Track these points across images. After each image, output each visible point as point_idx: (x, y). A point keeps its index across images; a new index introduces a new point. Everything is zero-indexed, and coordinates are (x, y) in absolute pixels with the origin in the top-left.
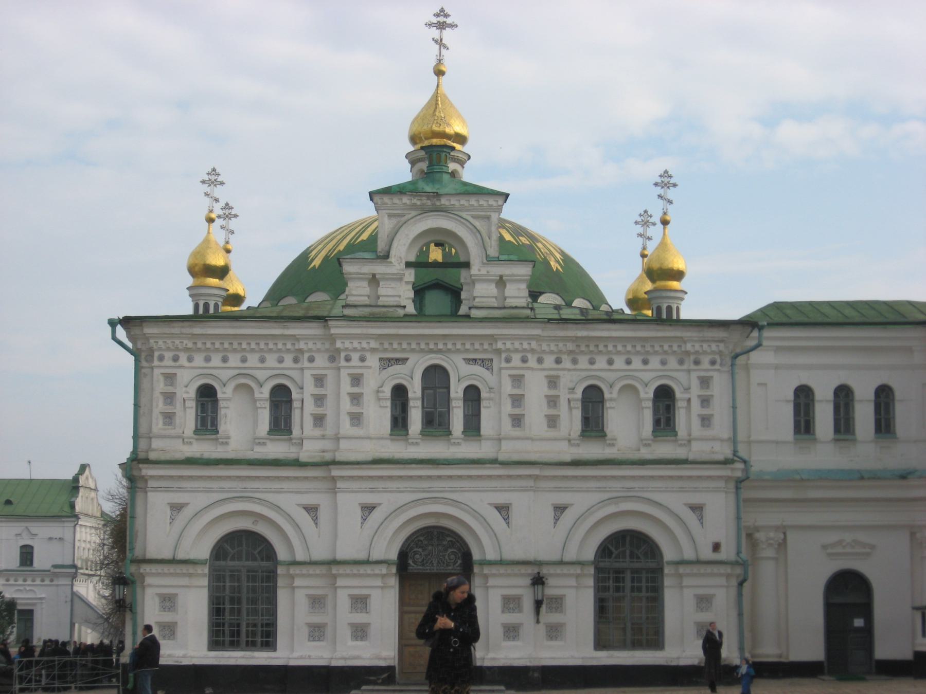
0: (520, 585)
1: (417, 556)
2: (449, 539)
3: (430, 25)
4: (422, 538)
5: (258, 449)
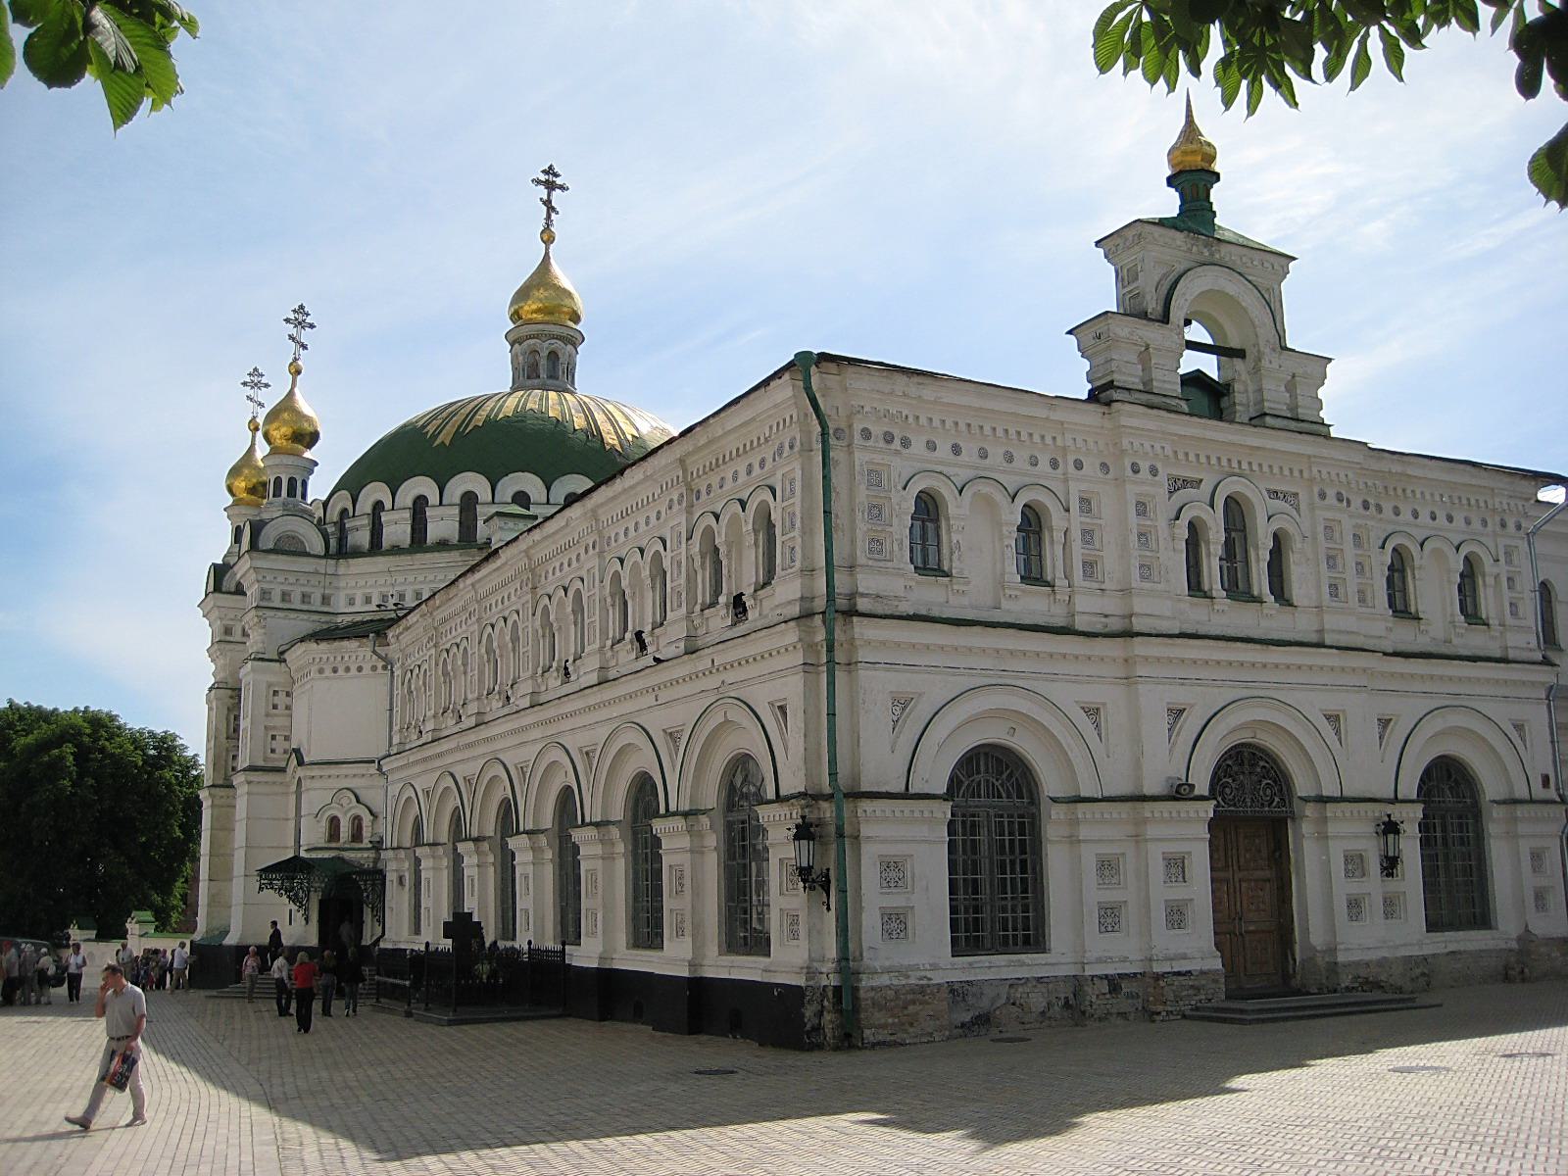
1: (1228, 791)
2: (1262, 763)
3: (538, 182)
4: (1229, 762)
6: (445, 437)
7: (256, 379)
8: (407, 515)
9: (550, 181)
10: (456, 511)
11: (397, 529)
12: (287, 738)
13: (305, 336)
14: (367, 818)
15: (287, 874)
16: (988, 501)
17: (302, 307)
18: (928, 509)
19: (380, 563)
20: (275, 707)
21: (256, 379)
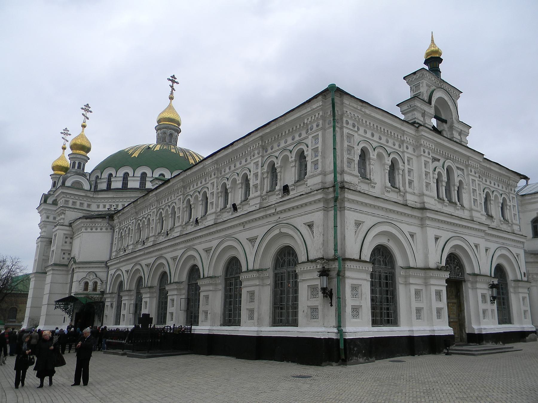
3: (169, 80)
5: (386, 194)
6: (136, 155)
7: (66, 132)
8: (122, 179)
9: (173, 80)
10: (139, 179)
11: (117, 184)
12: (69, 254)
13: (88, 115)
15: (67, 302)
17: (88, 105)
18: (364, 155)
19: (110, 195)
20: (66, 242)
21: (66, 132)
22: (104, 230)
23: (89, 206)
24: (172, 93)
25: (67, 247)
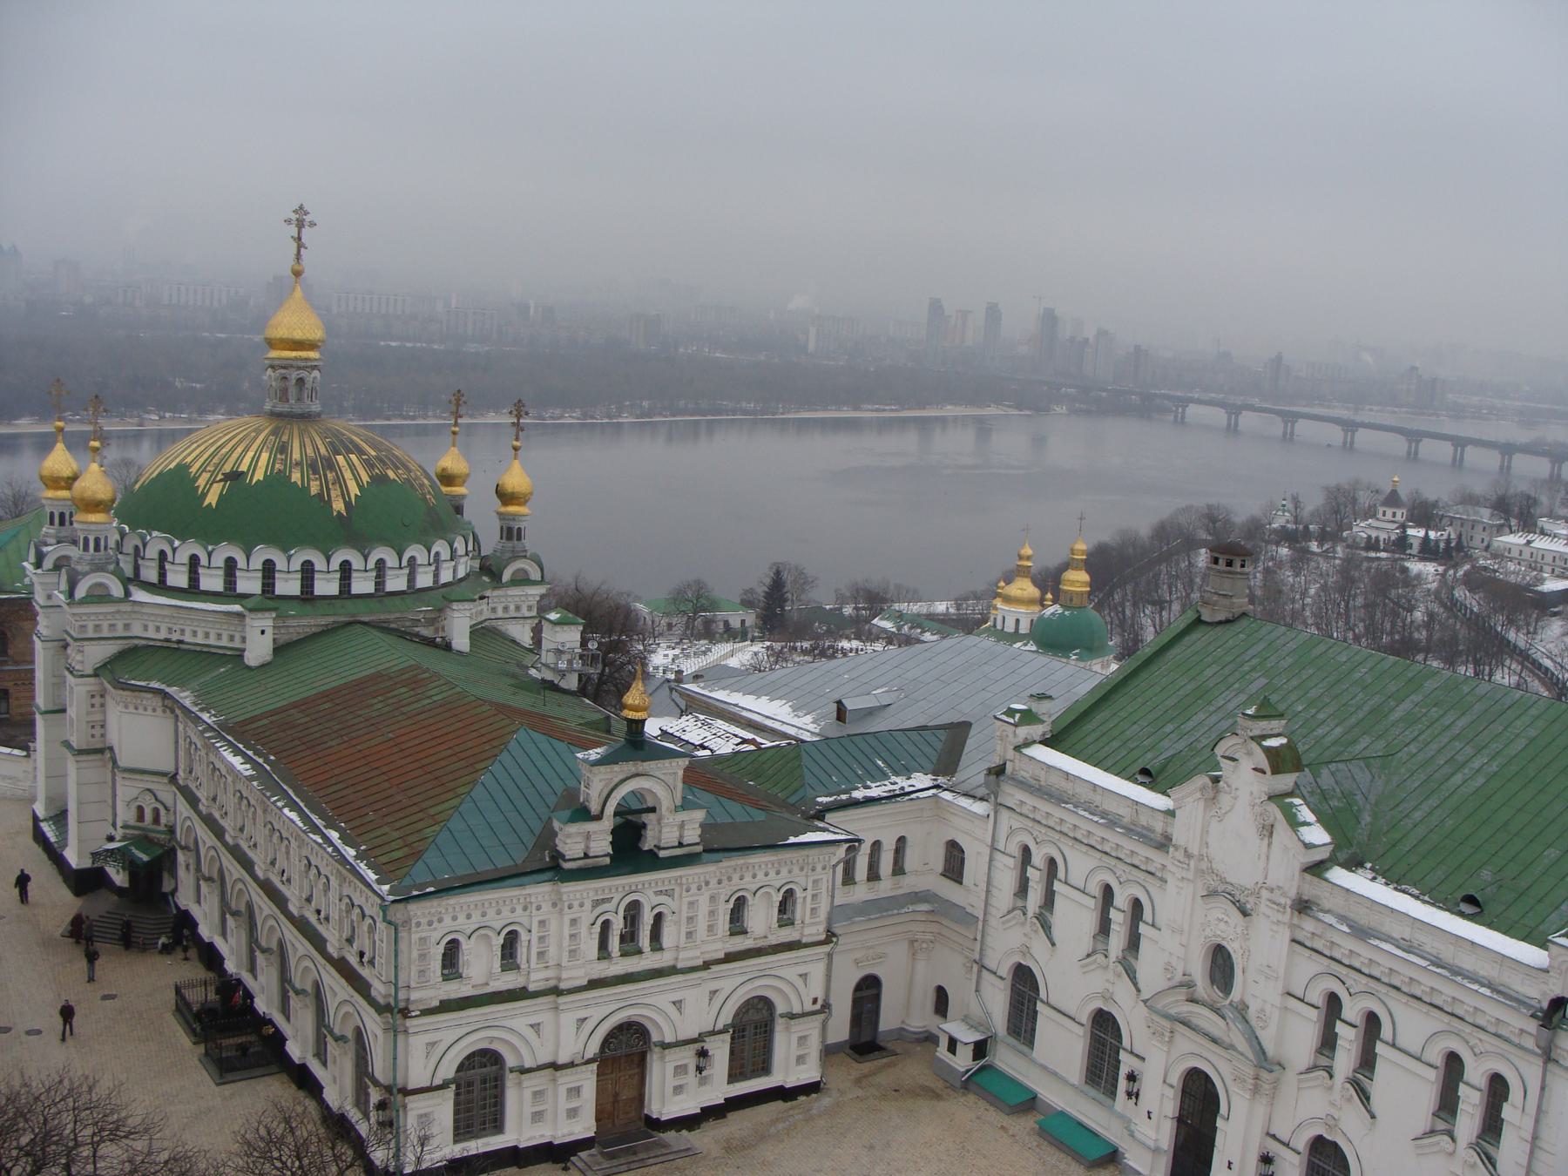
0: (687, 1056)
3: (288, 221)
8: (185, 569)
14: (163, 812)
16: (487, 936)
22: (159, 710)
23: (127, 626)
24: (298, 256)
25: (98, 717)
